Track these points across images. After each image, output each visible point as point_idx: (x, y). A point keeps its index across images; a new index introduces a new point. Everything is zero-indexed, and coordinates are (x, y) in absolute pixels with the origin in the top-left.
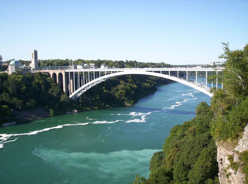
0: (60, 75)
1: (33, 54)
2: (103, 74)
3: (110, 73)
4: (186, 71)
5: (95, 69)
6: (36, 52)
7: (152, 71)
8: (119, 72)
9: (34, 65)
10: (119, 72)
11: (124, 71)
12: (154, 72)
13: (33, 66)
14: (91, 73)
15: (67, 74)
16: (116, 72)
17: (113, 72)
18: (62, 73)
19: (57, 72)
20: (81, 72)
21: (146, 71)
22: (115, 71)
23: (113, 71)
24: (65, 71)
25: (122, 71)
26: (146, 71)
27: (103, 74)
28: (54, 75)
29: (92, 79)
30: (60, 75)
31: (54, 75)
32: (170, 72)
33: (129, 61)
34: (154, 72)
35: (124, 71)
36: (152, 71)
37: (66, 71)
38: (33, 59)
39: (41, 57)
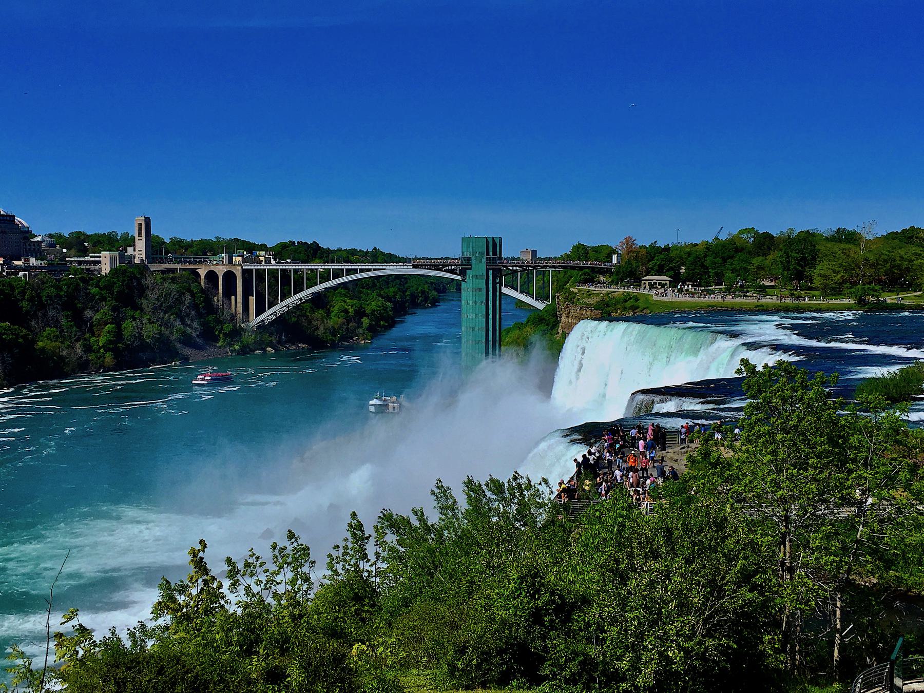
0: (230, 277)
2: (338, 274)
3: (357, 273)
8: (374, 270)
9: (144, 252)
10: (374, 270)
11: (385, 269)
13: (141, 254)
15: (246, 273)
16: (369, 270)
17: (362, 271)
19: (221, 270)
22: (367, 267)
23: (360, 267)
27: (338, 274)
28: (212, 276)
30: (230, 277)
31: (212, 276)
37: (244, 267)
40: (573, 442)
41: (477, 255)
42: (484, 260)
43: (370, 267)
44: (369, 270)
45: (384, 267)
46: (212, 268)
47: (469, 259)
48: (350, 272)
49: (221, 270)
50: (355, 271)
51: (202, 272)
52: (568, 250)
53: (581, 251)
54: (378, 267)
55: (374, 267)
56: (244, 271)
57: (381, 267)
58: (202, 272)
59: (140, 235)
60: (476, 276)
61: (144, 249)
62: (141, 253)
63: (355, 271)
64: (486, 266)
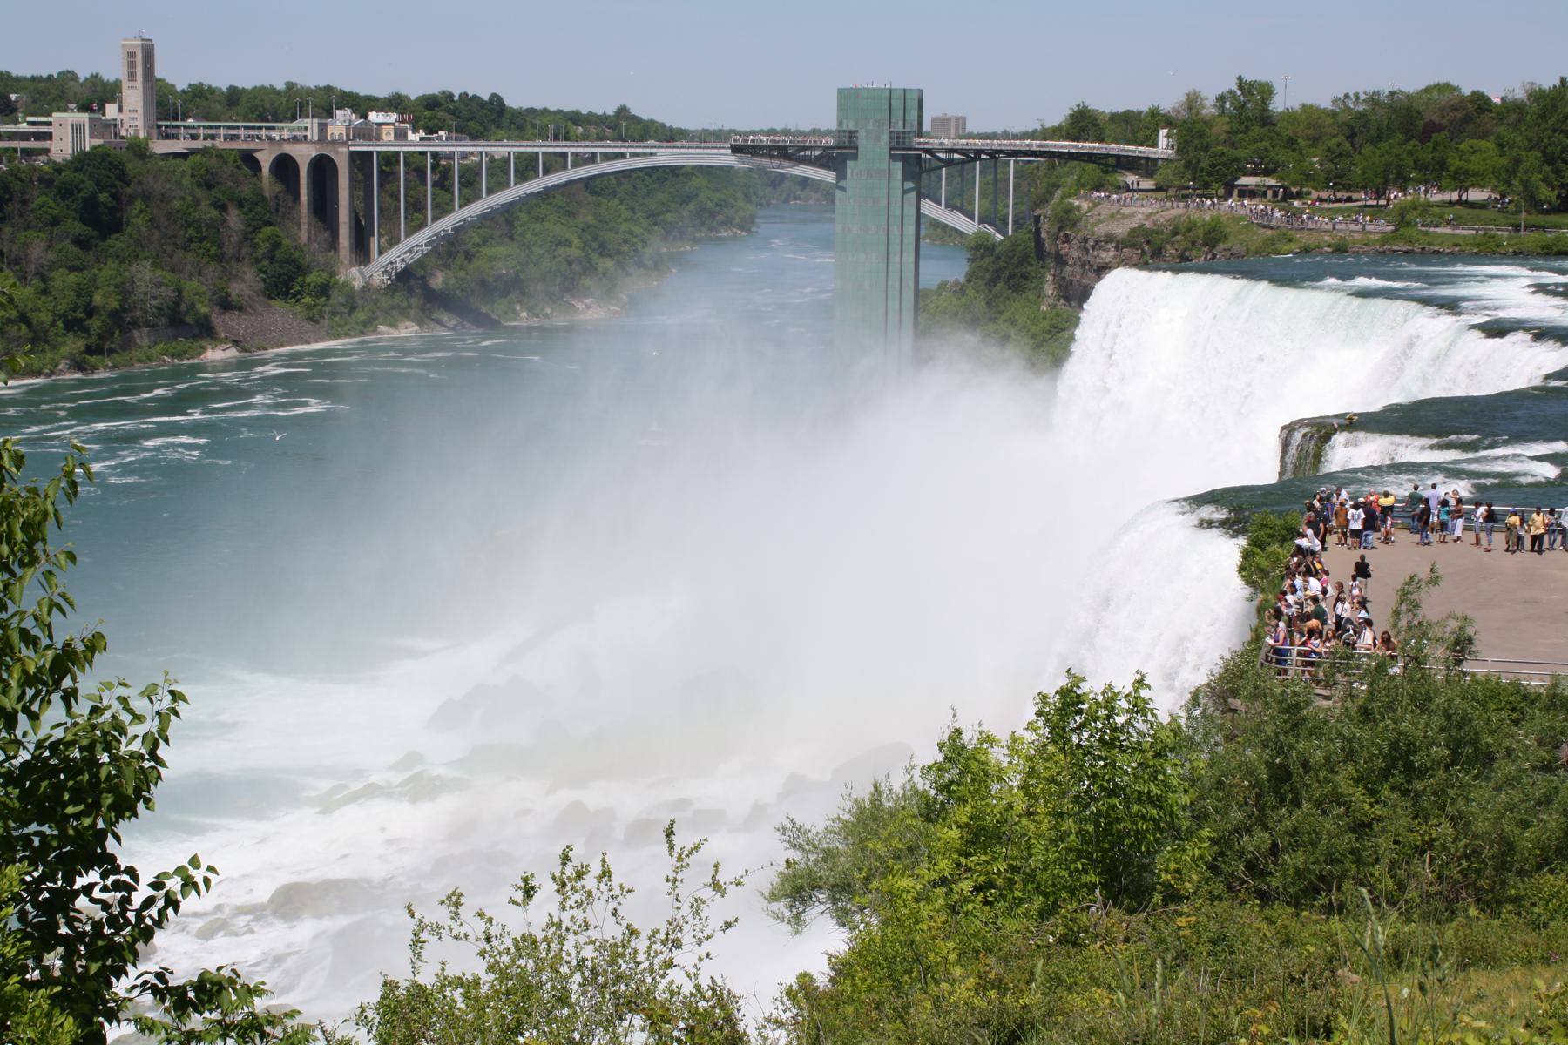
0: (323, 168)
1: (132, 55)
6: (149, 53)
8: (634, 155)
9: (140, 115)
10: (634, 155)
15: (360, 161)
16: (622, 156)
25: (651, 154)
27: (555, 163)
29: (496, 186)
30: (323, 168)
31: (284, 166)
33: (470, 95)
37: (352, 149)
38: (132, 84)
39: (178, 73)
40: (1207, 524)
41: (870, 127)
42: (885, 137)
43: (623, 150)
44: (622, 156)
46: (288, 149)
47: (852, 134)
48: (581, 160)
49: (304, 154)
50: (592, 158)
51: (265, 159)
52: (1057, 116)
53: (1083, 123)
55: (632, 150)
58: (265, 159)
59: (132, 76)
60: (868, 171)
61: (140, 107)
62: (133, 115)
63: (592, 158)
64: (891, 149)
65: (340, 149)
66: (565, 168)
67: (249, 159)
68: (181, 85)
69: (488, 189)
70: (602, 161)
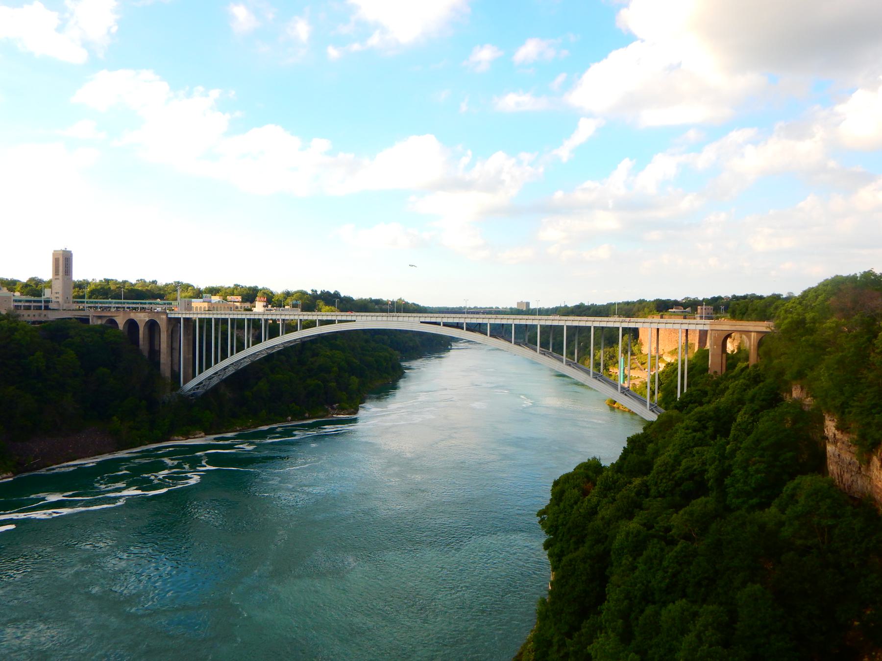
0: (152, 325)
2: (290, 327)
3: (315, 326)
4: (563, 326)
5: (301, 313)
7: (438, 324)
8: (340, 321)
10: (340, 321)
11: (355, 321)
12: (445, 325)
14: (255, 324)
18: (158, 322)
19: (142, 318)
20: (274, 321)
21: (421, 322)
22: (329, 318)
23: (320, 318)
24: (167, 314)
26: (421, 322)
27: (290, 327)
30: (152, 325)
31: (132, 325)
32: (567, 329)
33: (319, 293)
34: (445, 325)
35: (355, 321)
36: (438, 324)
37: (169, 316)
38: (57, 277)
43: (334, 318)
45: (354, 318)
49: (142, 318)
50: (311, 324)
51: (121, 321)
54: (344, 318)
55: (339, 318)
56: (170, 320)
57: (349, 318)
58: (121, 321)
62: (57, 295)
65: (162, 316)
66: (297, 330)
67: (112, 322)
68: (121, 281)
69: (253, 342)
70: (321, 325)
